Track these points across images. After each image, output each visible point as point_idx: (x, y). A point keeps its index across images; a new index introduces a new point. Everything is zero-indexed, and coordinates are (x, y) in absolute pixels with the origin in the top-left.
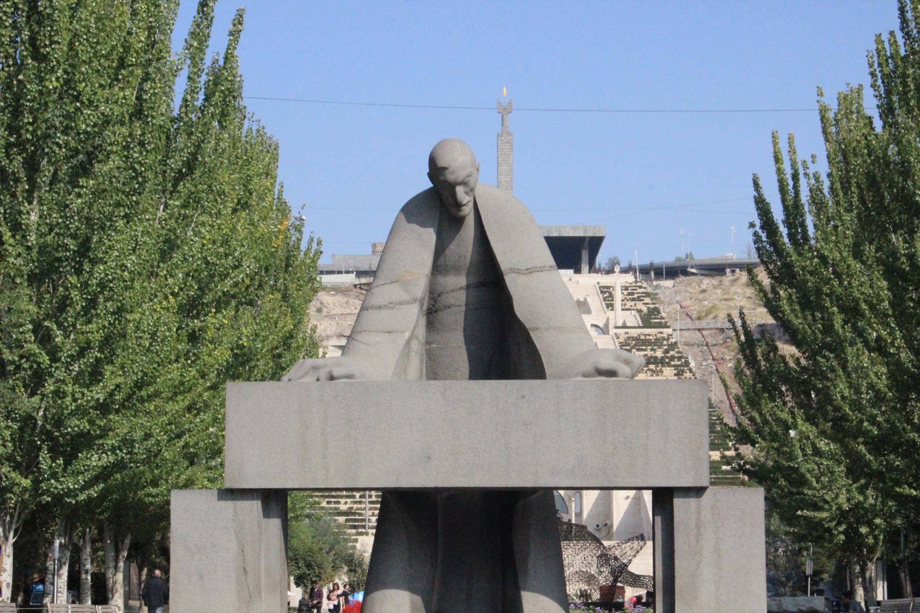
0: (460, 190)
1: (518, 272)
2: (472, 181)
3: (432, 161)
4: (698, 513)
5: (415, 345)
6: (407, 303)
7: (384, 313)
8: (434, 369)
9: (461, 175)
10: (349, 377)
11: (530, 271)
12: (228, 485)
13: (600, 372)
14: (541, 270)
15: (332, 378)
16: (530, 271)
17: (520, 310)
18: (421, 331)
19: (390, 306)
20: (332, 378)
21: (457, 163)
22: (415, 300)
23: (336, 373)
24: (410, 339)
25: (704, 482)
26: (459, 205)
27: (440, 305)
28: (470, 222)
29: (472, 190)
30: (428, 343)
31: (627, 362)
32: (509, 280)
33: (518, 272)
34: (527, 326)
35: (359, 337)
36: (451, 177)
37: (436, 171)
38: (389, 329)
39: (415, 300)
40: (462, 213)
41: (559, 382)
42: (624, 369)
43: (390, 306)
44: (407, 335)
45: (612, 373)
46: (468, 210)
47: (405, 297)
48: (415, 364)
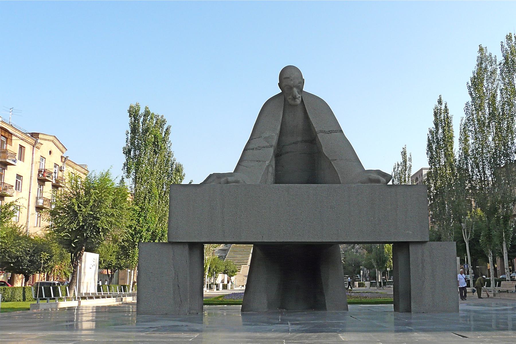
1: (325, 132)
5: (271, 170)
6: (267, 147)
7: (255, 152)
11: (330, 132)
13: (371, 181)
16: (330, 132)
19: (259, 148)
24: (268, 167)
25: (427, 239)
33: (325, 132)
38: (258, 160)
39: (271, 146)
43: (259, 148)
45: (378, 181)
47: (267, 144)
48: (271, 178)
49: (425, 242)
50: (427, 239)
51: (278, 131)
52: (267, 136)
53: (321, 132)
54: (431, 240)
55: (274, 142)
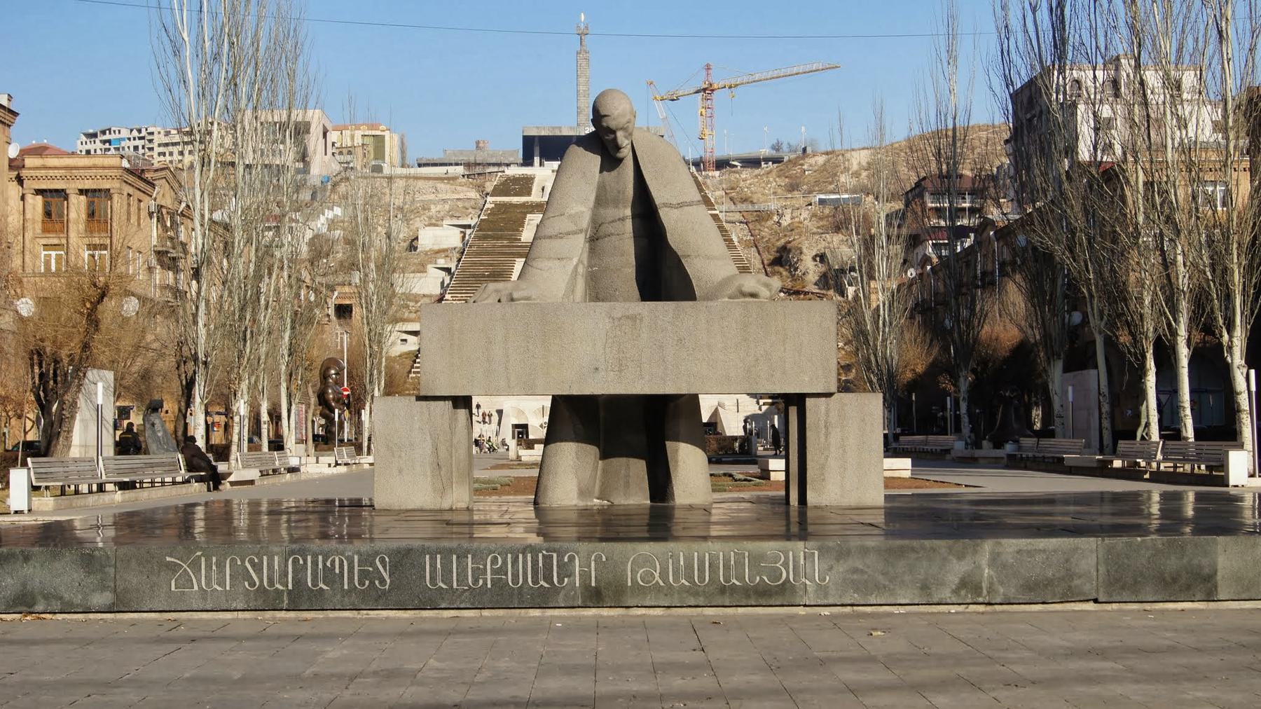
0: (620, 134)
1: (670, 206)
2: (630, 125)
3: (596, 111)
4: (827, 414)
5: (581, 270)
6: (575, 233)
7: (556, 243)
8: (597, 291)
9: (623, 121)
10: (528, 299)
11: (680, 205)
12: (423, 393)
14: (690, 204)
15: (512, 300)
16: (680, 205)
17: (673, 240)
18: (585, 255)
19: (559, 236)
20: (512, 300)
21: (617, 112)
22: (581, 231)
23: (515, 296)
24: (576, 267)
25: (833, 389)
26: (618, 148)
27: (601, 234)
28: (629, 162)
29: (631, 134)
30: (590, 266)
31: (767, 286)
32: (664, 214)
33: (670, 206)
34: (679, 254)
35: (534, 264)
36: (612, 124)
37: (598, 117)
39: (581, 231)
40: (620, 155)
41: (710, 303)
42: (764, 292)
44: (575, 261)
45: (753, 295)
46: (626, 153)
47: (574, 228)
49: (828, 395)
50: (833, 389)
51: (591, 203)
52: (573, 212)
53: (665, 205)
54: (845, 387)
55: (585, 222)
